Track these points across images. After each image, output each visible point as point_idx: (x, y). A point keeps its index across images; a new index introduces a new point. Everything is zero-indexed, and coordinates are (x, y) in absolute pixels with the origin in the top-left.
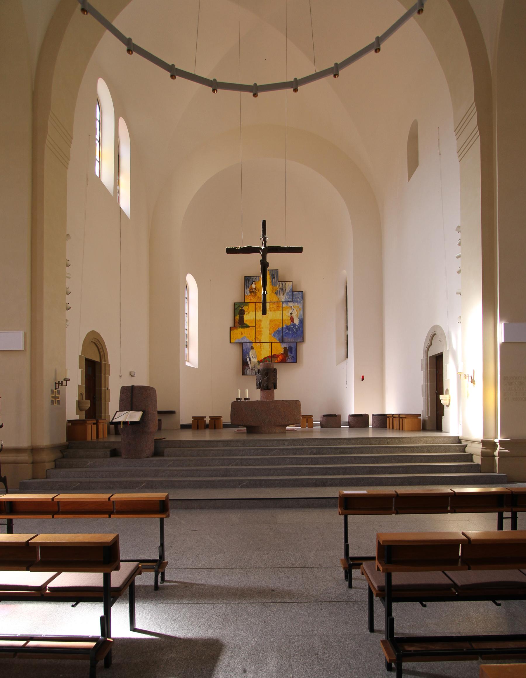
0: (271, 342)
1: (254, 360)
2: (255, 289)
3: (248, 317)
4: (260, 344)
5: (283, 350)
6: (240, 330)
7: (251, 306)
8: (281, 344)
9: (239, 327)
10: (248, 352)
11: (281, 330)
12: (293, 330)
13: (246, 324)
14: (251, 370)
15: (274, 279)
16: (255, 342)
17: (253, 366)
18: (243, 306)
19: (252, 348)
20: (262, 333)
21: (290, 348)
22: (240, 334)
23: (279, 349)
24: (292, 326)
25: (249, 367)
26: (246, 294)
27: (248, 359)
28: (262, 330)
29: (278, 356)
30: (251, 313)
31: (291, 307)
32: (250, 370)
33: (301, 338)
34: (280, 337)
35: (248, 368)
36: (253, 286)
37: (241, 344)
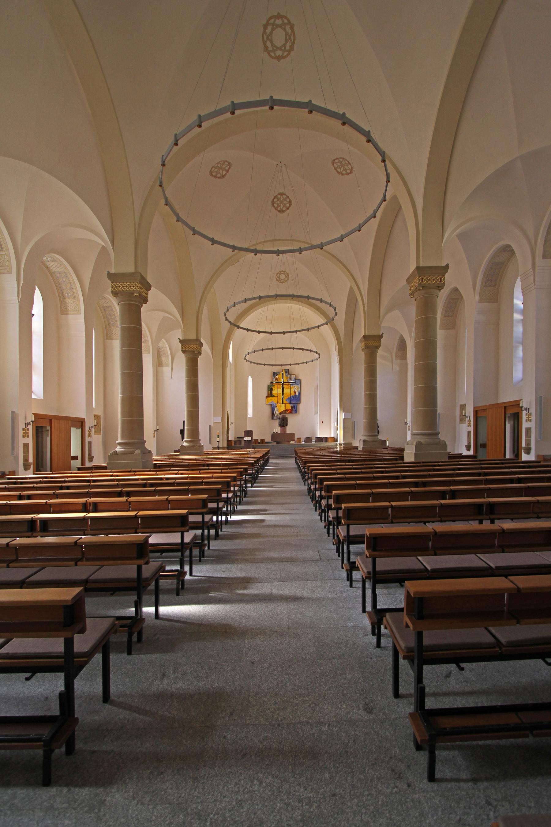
1: (277, 412)
3: (274, 392)
6: (271, 398)
7: (276, 387)
19: (276, 406)
21: (294, 406)
22: (271, 400)
23: (289, 407)
29: (288, 410)
36: (277, 377)
37: (271, 405)
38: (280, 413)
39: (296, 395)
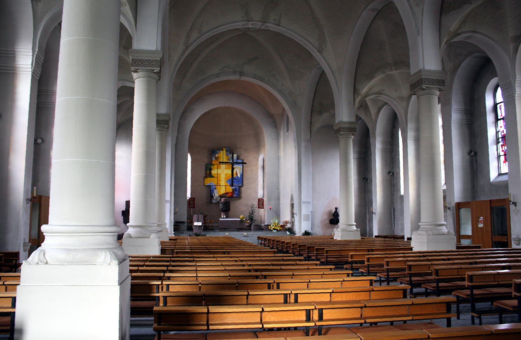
0: (226, 186)
2: (218, 157)
3: (214, 172)
5: (232, 190)
6: (209, 178)
7: (216, 166)
16: (217, 186)
17: (216, 197)
19: (216, 188)
21: (236, 189)
27: (213, 194)
29: (229, 193)
30: (215, 170)
36: (217, 156)
38: (221, 196)
39: (238, 177)
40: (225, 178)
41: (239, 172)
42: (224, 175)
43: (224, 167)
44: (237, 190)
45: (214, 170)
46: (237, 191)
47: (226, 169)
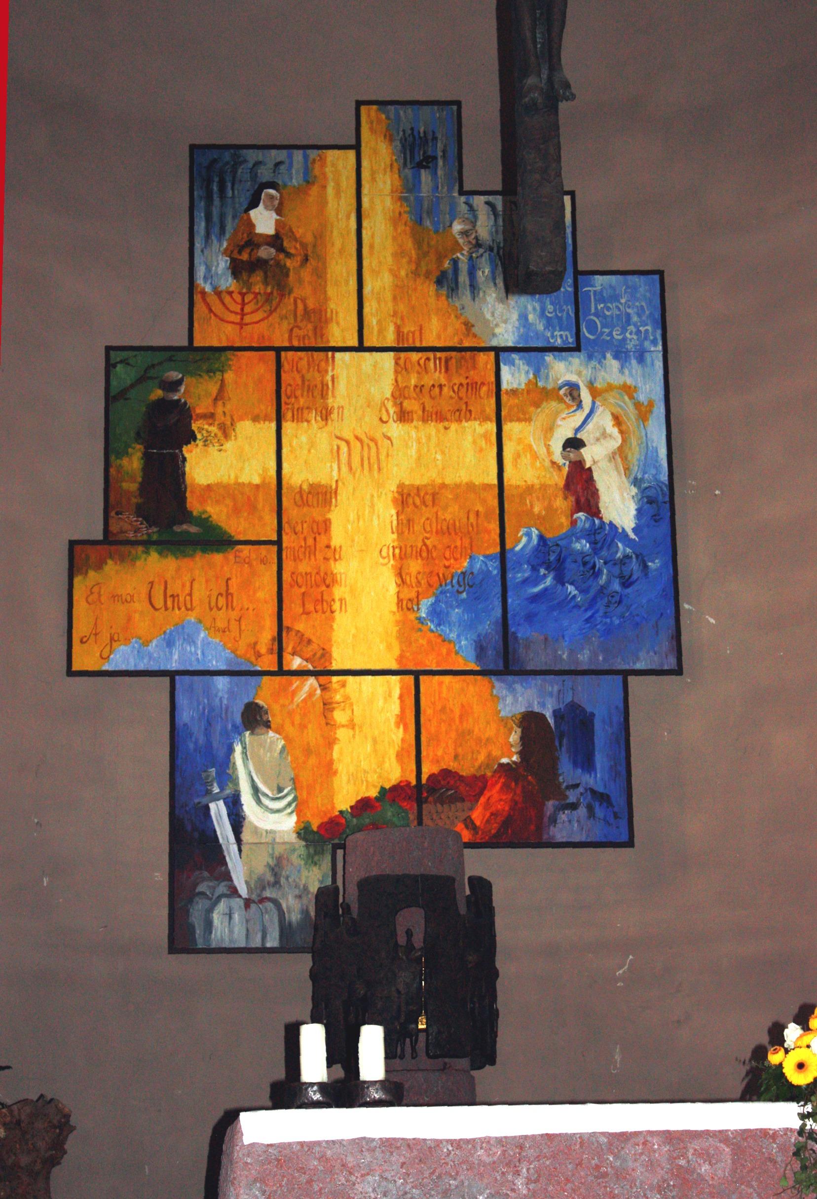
0: (417, 674)
2: (276, 241)
4: (324, 688)
5: (514, 737)
8: (499, 687)
9: (147, 544)
10: (221, 753)
11: (494, 568)
12: (597, 574)
13: (205, 523)
14: (248, 903)
15: (425, 176)
16: (281, 671)
17: (261, 863)
18: (175, 375)
20: (338, 592)
24: (582, 545)
25: (227, 876)
26: (200, 281)
27: (218, 810)
28: (338, 568)
30: (245, 427)
31: (573, 389)
32: (237, 903)
33: (665, 643)
34: (488, 626)
35: (222, 888)
40: (402, 556)
41: (621, 452)
42: (388, 512)
43: (385, 387)
44: (601, 734)
45: (226, 432)
46: (600, 760)
47: (403, 416)
